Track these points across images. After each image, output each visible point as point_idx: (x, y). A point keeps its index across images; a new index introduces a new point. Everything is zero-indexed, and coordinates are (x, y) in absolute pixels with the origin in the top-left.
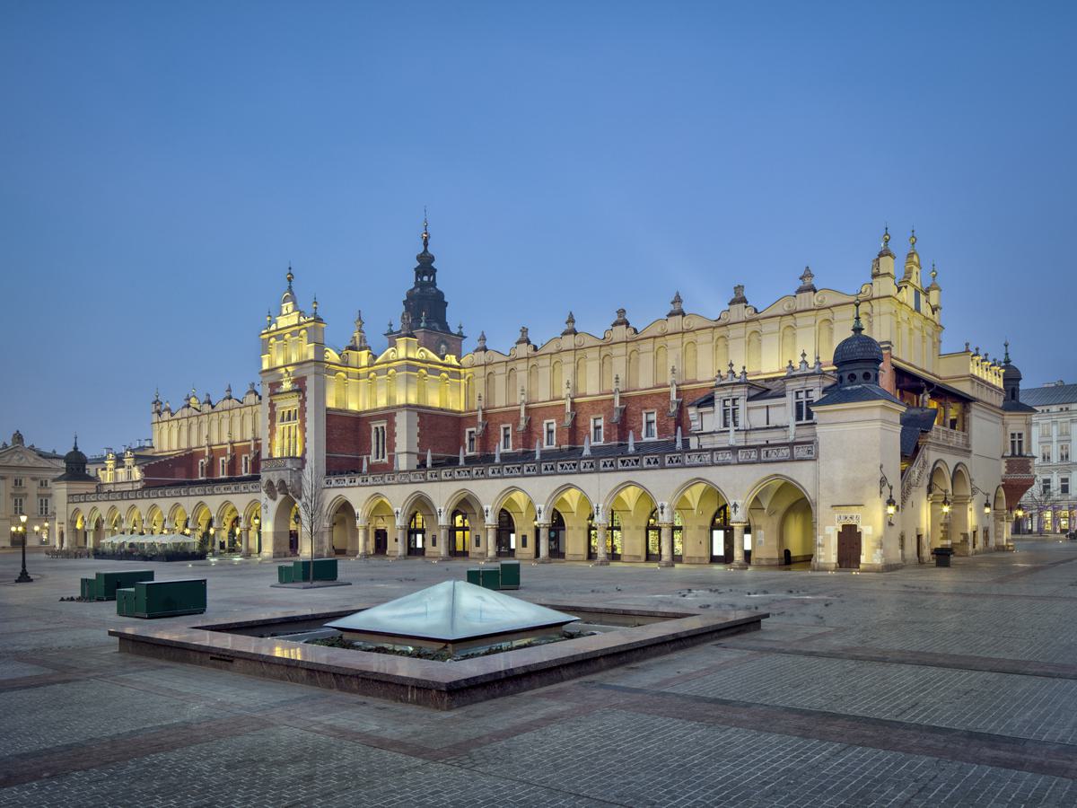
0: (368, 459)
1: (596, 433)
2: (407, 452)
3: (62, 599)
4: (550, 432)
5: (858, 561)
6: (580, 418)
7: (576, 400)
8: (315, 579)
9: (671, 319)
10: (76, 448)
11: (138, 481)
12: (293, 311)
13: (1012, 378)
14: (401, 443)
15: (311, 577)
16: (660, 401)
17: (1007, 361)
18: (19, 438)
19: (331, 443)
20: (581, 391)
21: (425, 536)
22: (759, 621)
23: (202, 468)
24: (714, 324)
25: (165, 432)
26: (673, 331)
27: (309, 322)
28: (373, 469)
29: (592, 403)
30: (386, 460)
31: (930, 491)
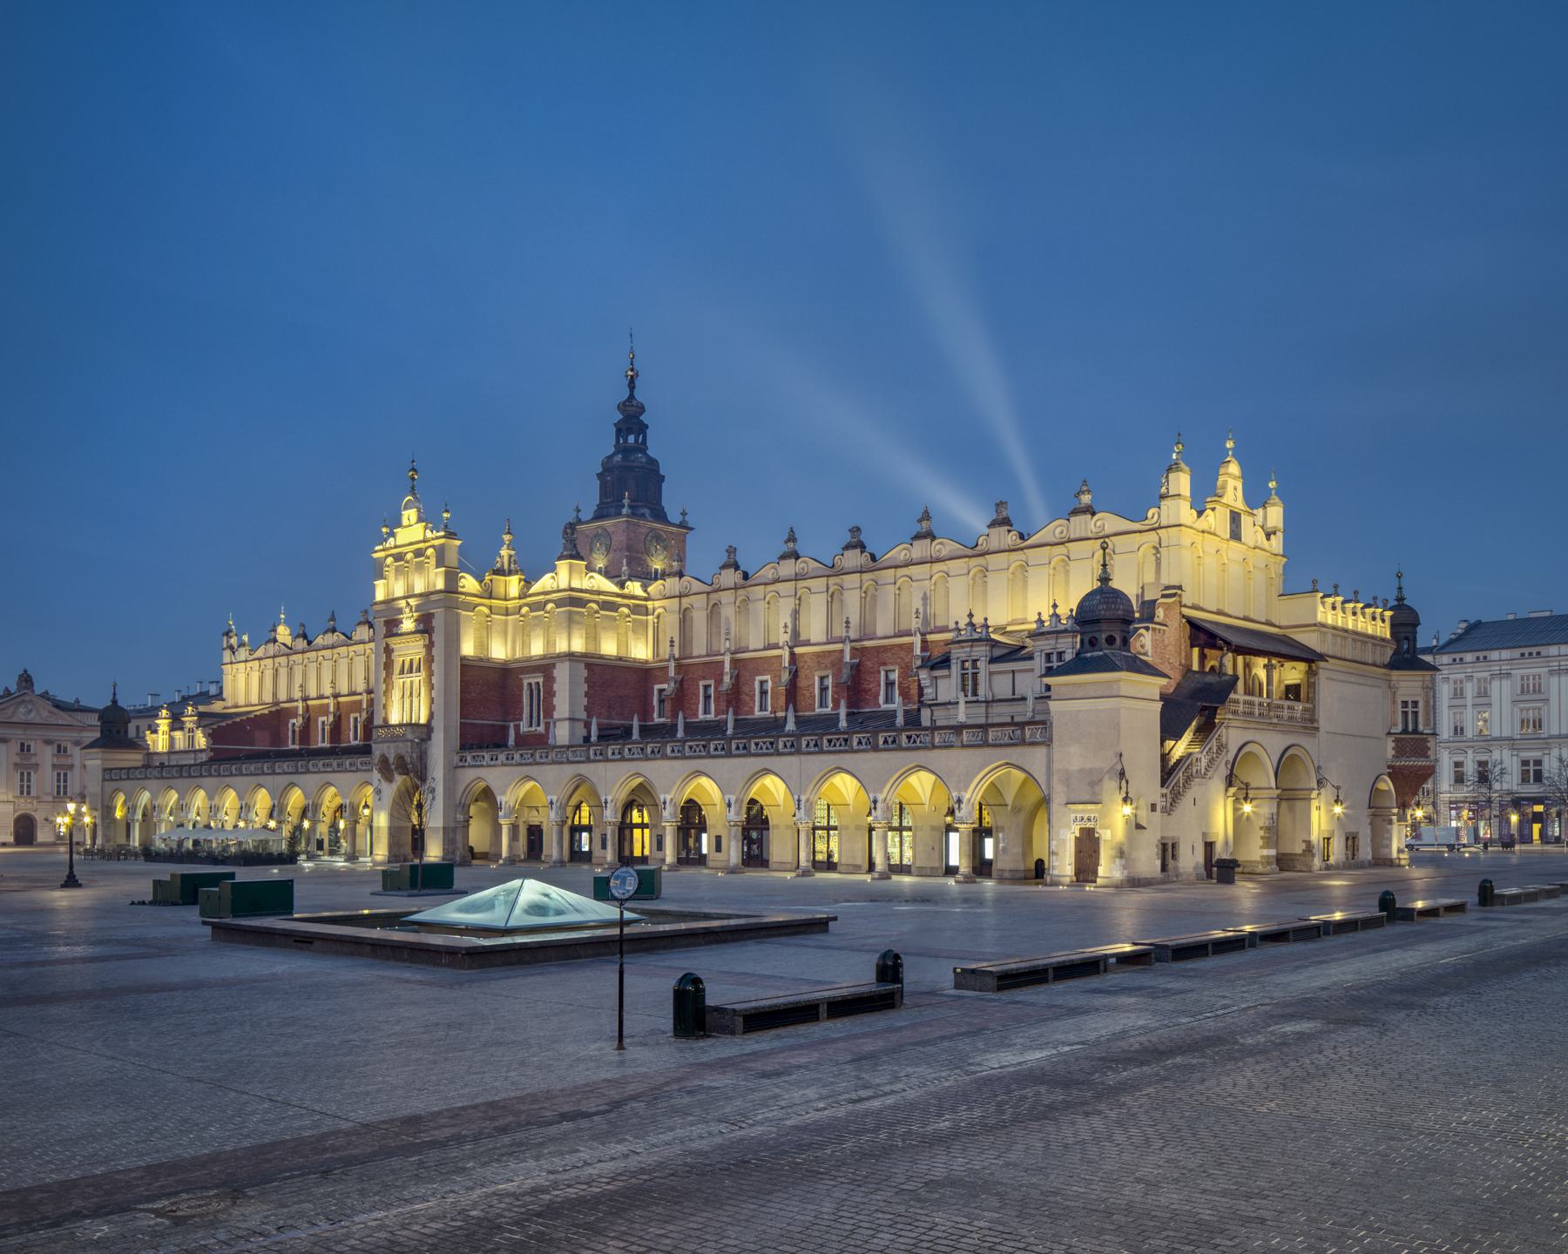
0: (517, 728)
1: (822, 700)
2: (570, 719)
3: (133, 903)
4: (763, 693)
5: (1095, 873)
6: (802, 674)
7: (798, 650)
8: (424, 886)
9: (916, 543)
10: (114, 702)
11: (201, 751)
12: (417, 522)
13: (1405, 622)
14: (562, 706)
15: (419, 885)
16: (903, 654)
17: (1400, 599)
18: (26, 681)
19: (467, 705)
20: (803, 637)
21: (593, 834)
22: (827, 923)
23: (294, 732)
24: (970, 552)
25: (242, 677)
26: (920, 561)
27: (437, 538)
28: (524, 741)
29: (818, 655)
30: (541, 729)
31: (1230, 784)
